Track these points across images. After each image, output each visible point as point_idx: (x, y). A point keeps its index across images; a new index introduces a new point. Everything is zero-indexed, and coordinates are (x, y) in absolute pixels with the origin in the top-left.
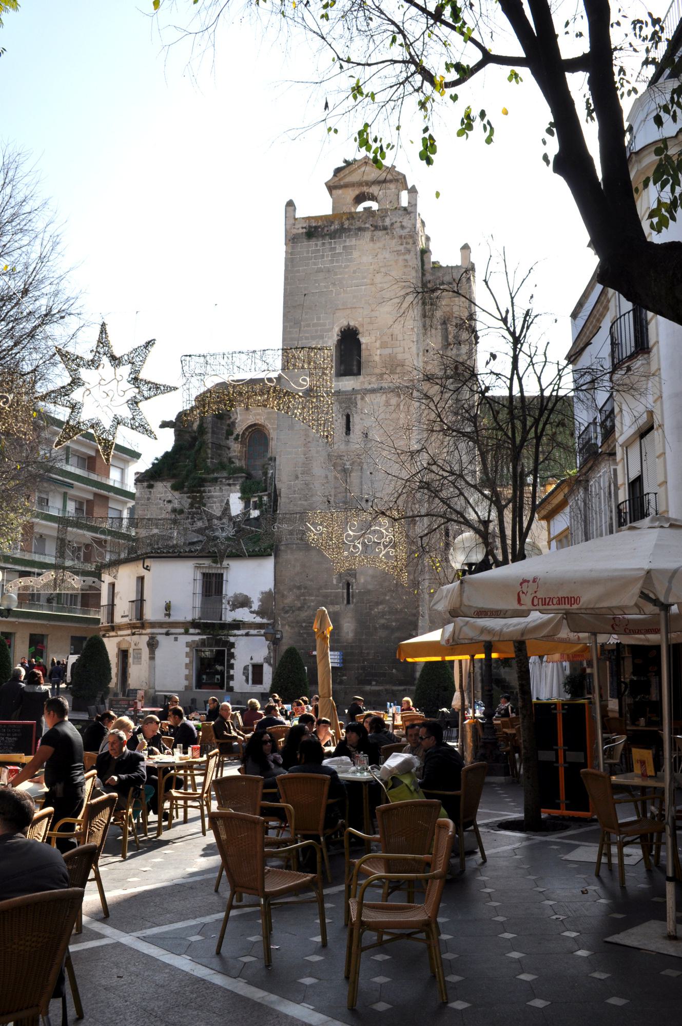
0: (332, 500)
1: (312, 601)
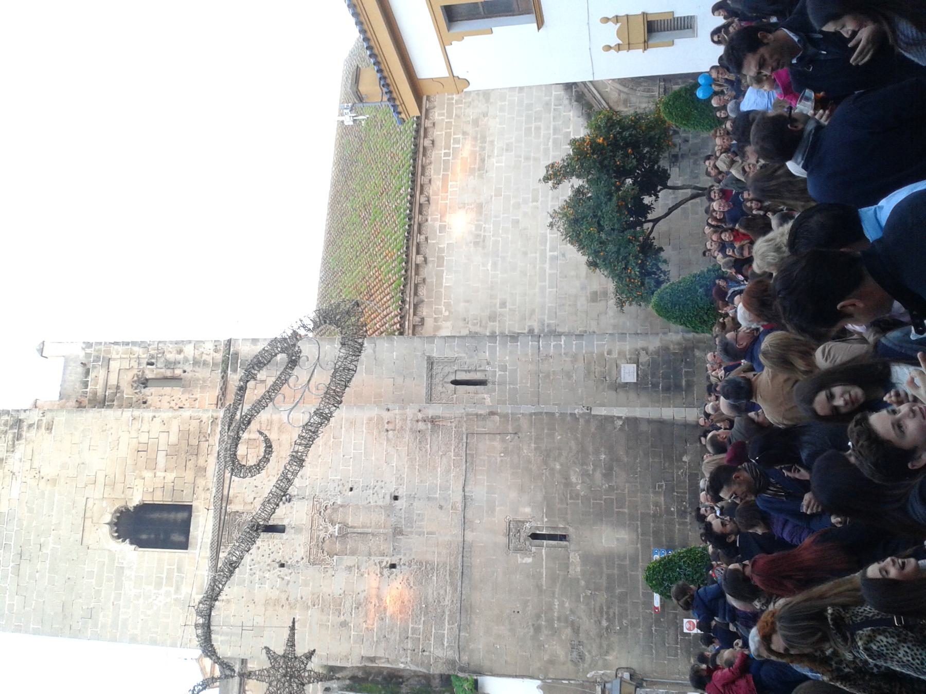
0: (388, 560)
1: (562, 604)
